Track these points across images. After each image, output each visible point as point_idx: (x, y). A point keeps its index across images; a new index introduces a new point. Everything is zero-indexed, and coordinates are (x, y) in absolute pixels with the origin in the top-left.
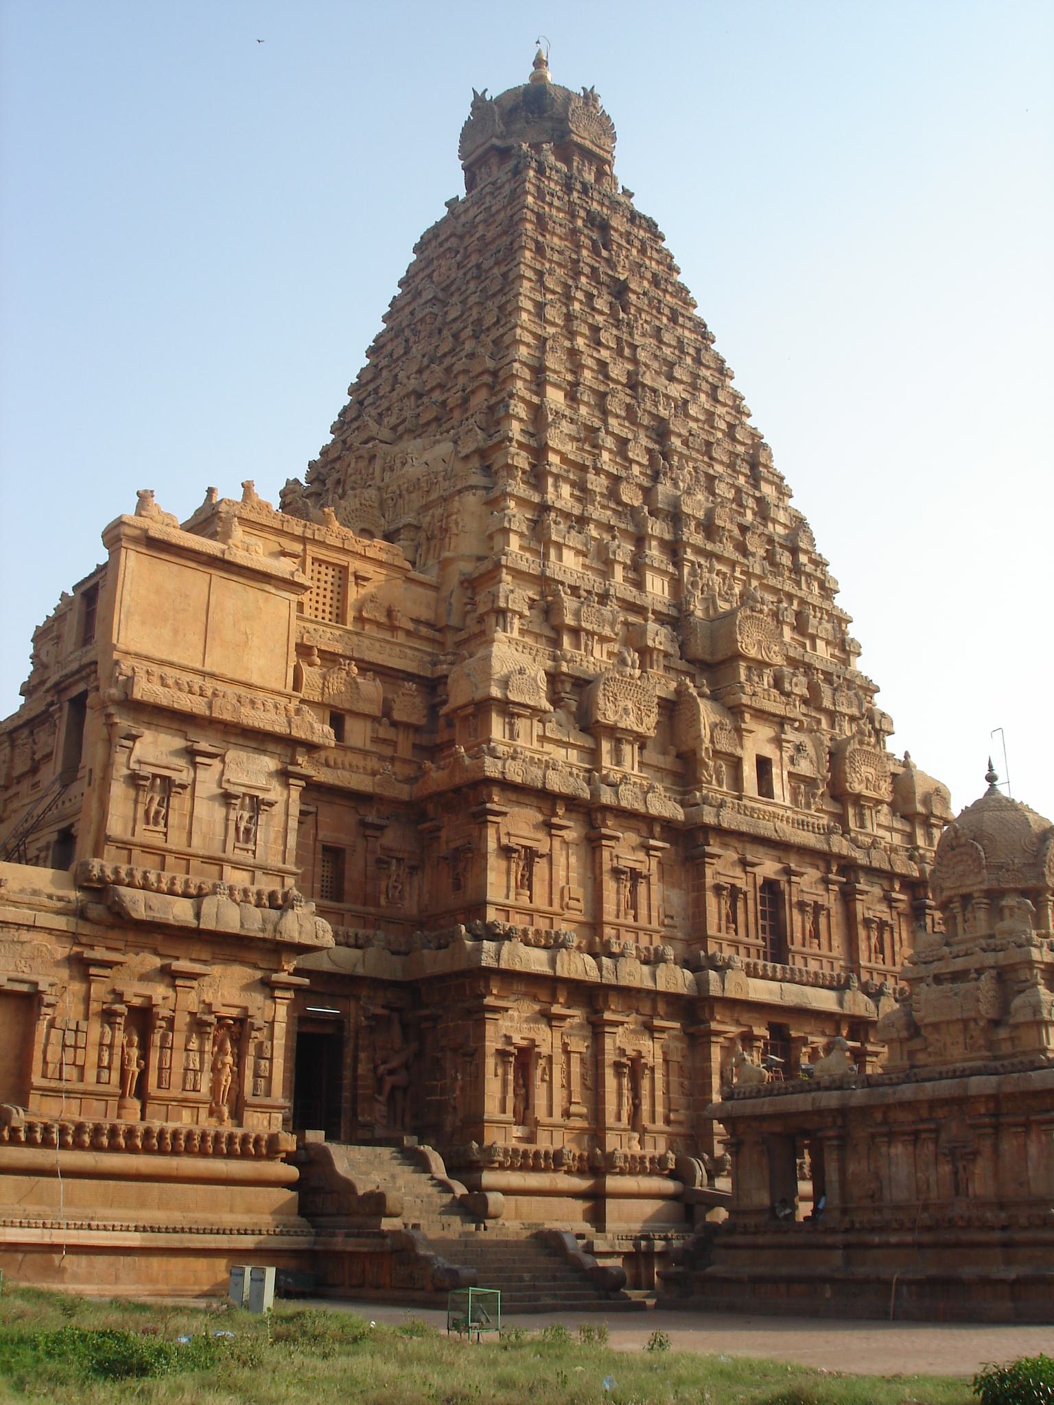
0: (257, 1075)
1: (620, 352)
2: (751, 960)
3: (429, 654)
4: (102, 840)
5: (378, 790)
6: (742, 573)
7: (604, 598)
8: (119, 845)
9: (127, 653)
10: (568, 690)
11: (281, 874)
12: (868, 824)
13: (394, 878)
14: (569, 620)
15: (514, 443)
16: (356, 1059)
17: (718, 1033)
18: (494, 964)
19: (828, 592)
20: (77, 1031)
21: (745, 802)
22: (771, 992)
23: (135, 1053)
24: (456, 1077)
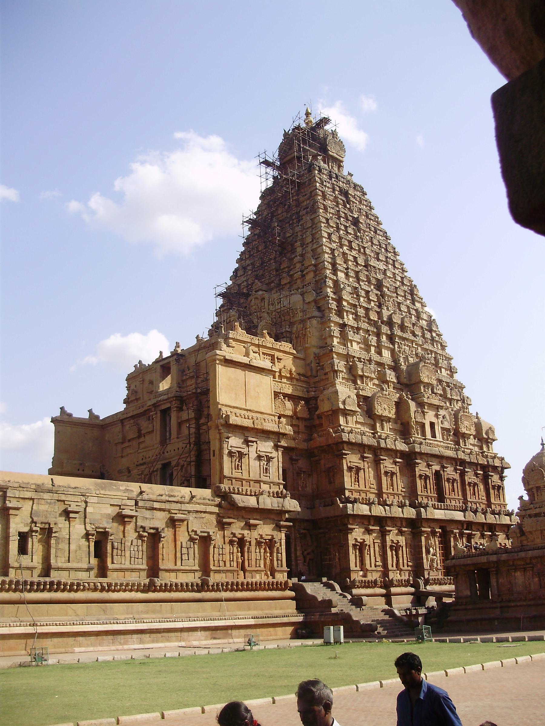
0: (277, 560)
1: (359, 251)
2: (433, 503)
3: (305, 388)
4: (222, 477)
6: (416, 344)
7: (370, 361)
9: (223, 405)
11: (279, 484)
12: (467, 444)
14: (360, 373)
15: (330, 298)
16: (296, 550)
17: (424, 532)
18: (352, 513)
19: (443, 347)
20: (222, 548)
21: (427, 441)
22: (441, 515)
23: (240, 554)
24: (336, 555)
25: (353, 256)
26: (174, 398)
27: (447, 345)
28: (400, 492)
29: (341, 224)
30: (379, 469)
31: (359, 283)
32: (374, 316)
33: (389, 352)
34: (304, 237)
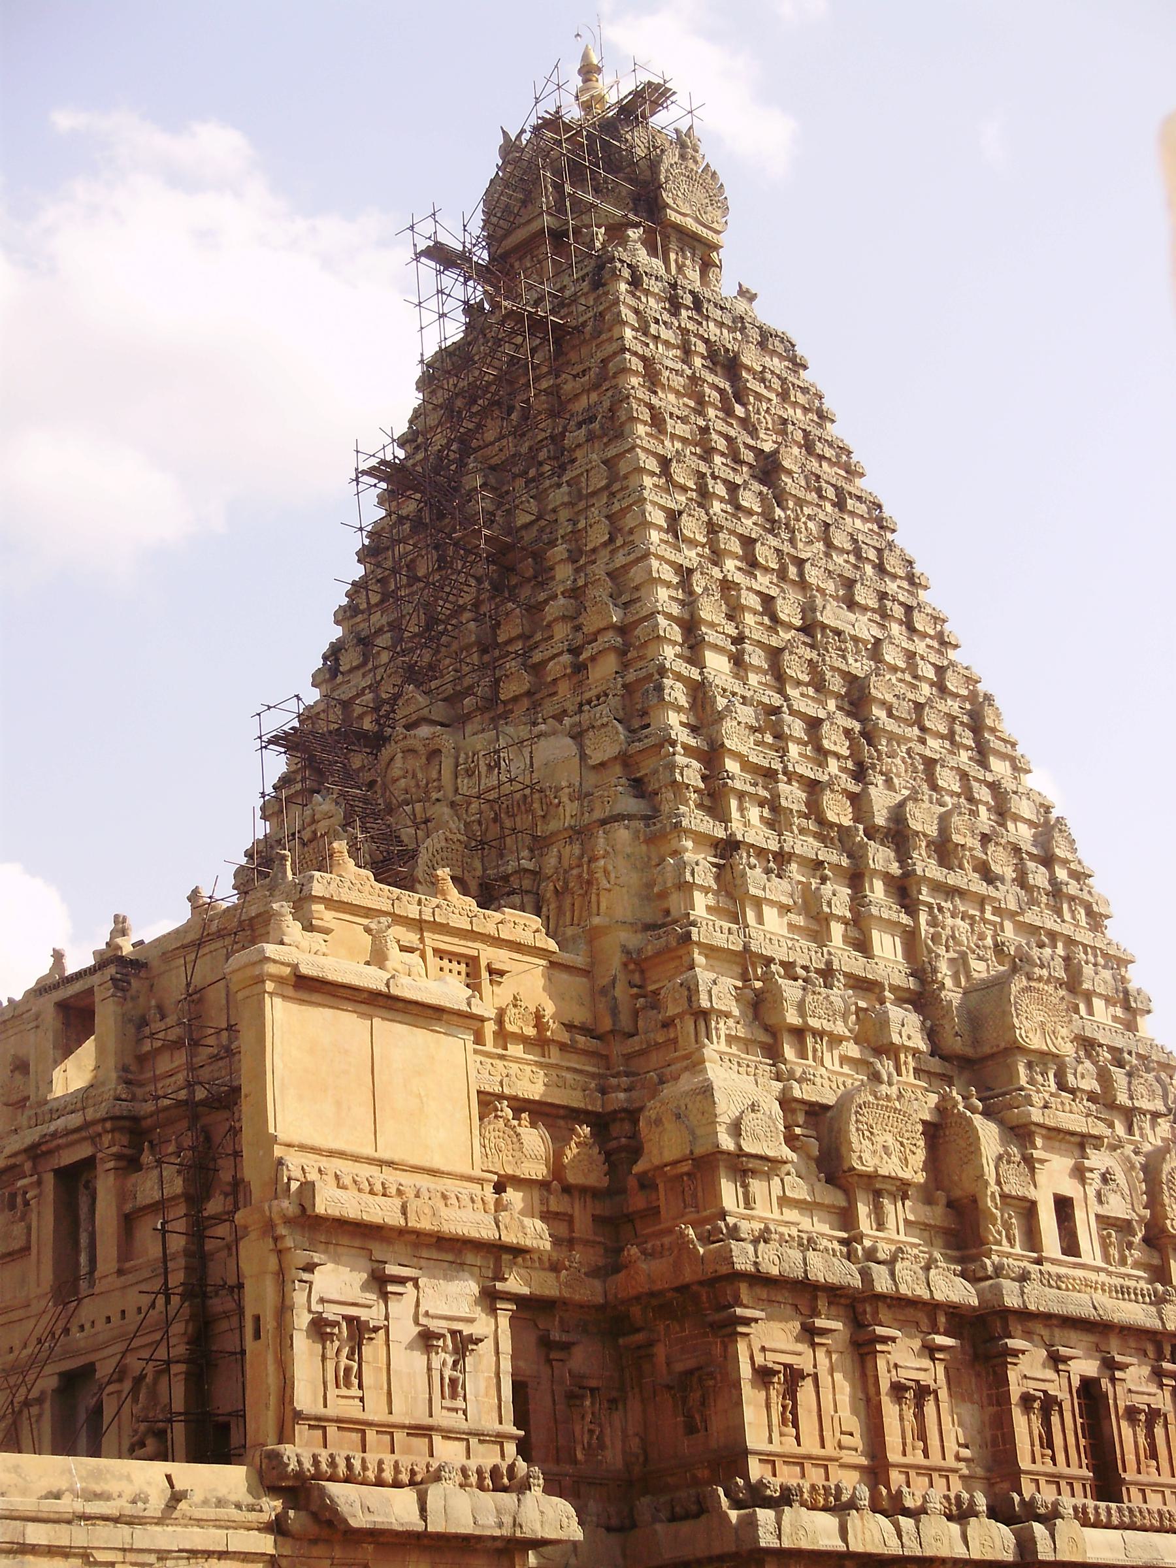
1: (782, 574)
2: (1079, 1501)
3: (593, 1076)
5: (566, 1294)
6: (997, 911)
7: (827, 973)
8: (312, 1423)
9: (289, 1145)
10: (801, 1123)
11: (500, 1439)
13: (589, 1418)
14: (792, 1018)
15: (679, 748)
18: (774, 1543)
19: (1096, 920)
21: (1047, 1267)
22: (1111, 1548)
25: (759, 593)
26: (108, 1125)
27: (1112, 910)
28: (951, 1462)
29: (715, 477)
30: (870, 1373)
31: (781, 691)
32: (838, 812)
33: (897, 940)
34: (582, 525)
